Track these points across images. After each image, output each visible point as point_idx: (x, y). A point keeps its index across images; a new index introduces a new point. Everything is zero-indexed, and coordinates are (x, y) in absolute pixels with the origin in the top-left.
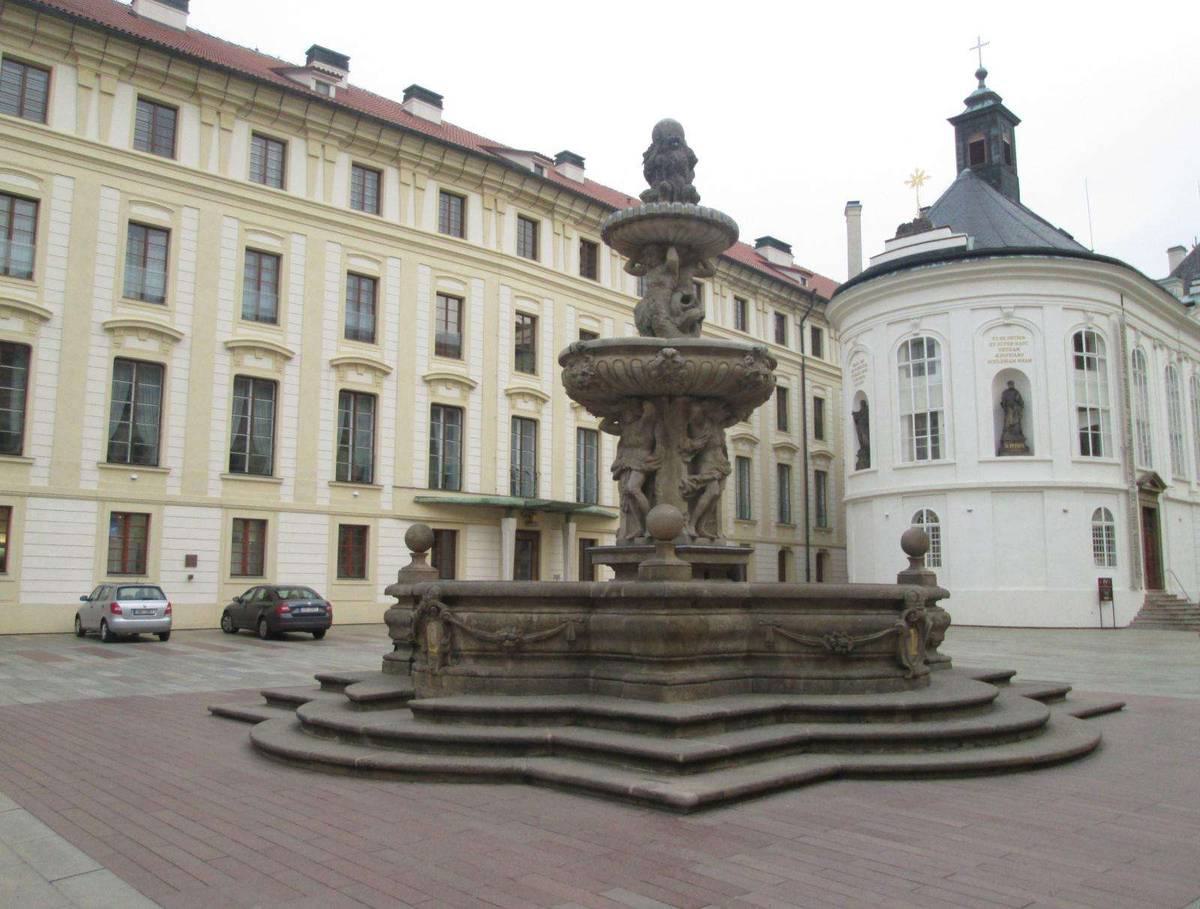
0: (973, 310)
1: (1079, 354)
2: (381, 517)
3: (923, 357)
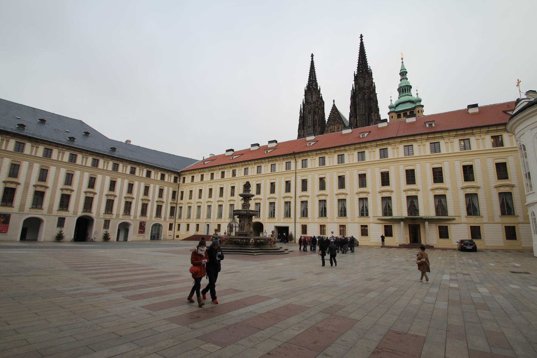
2: (370, 223)
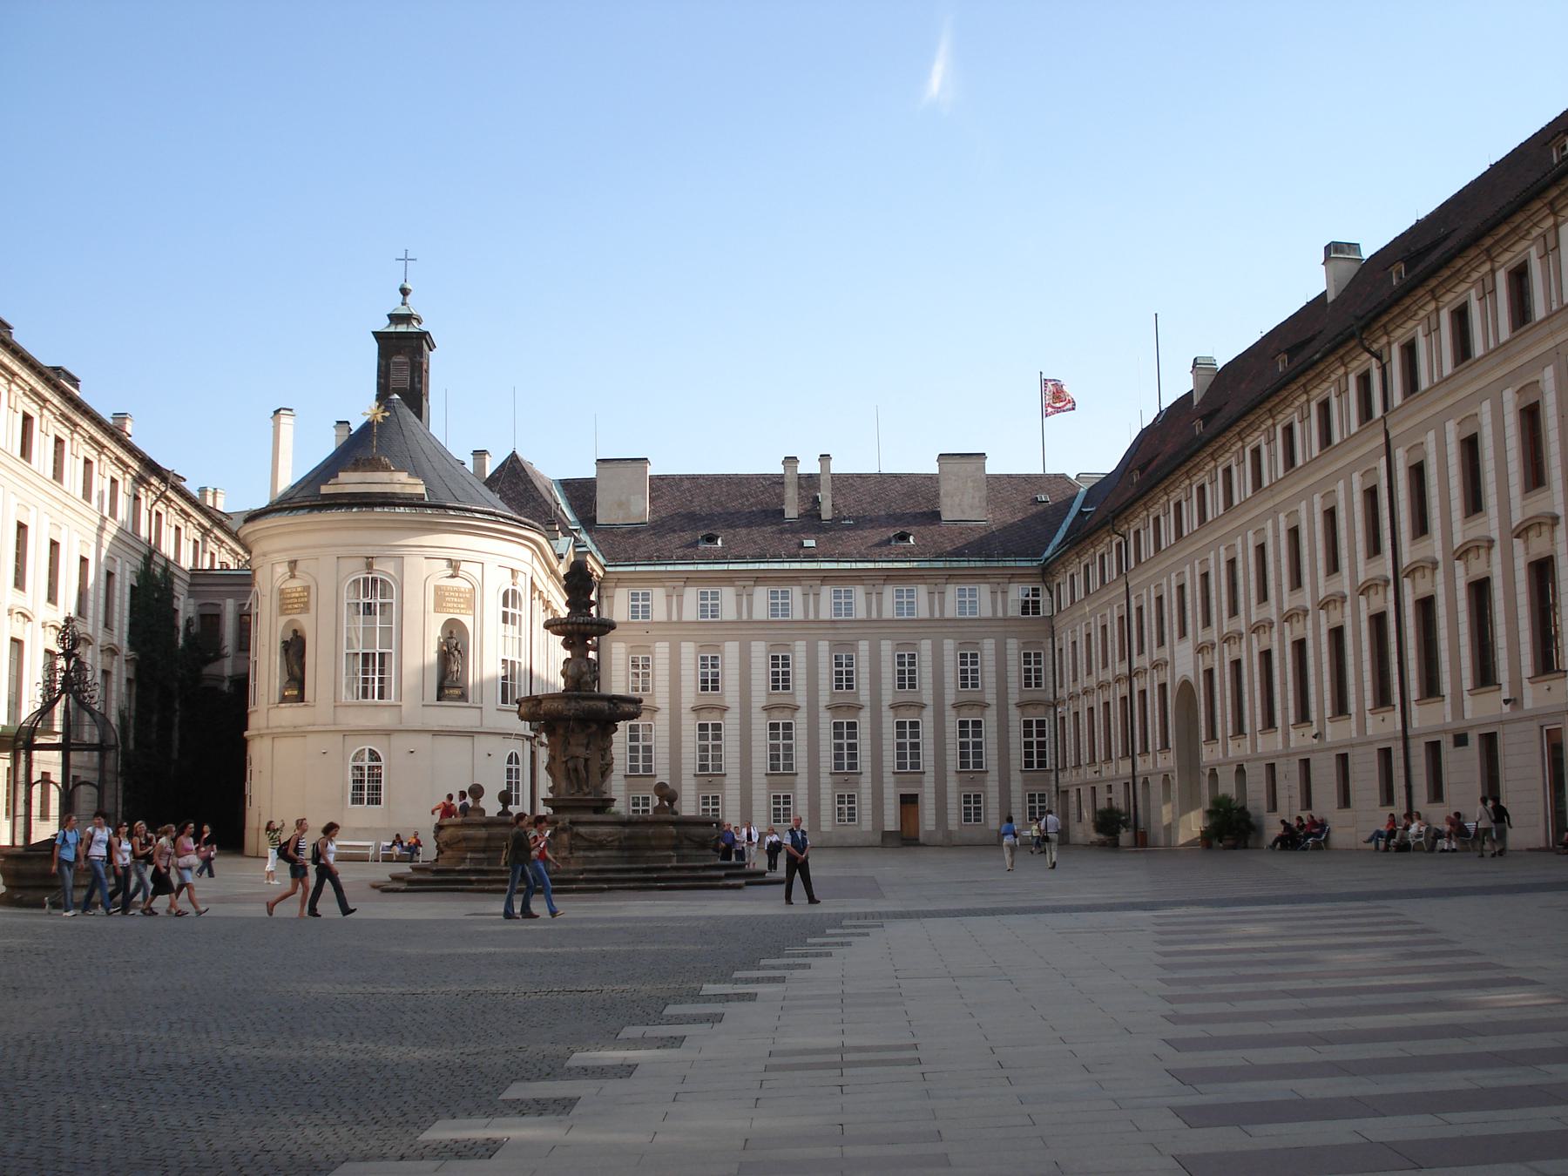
0: (426, 558)
1: (505, 609)
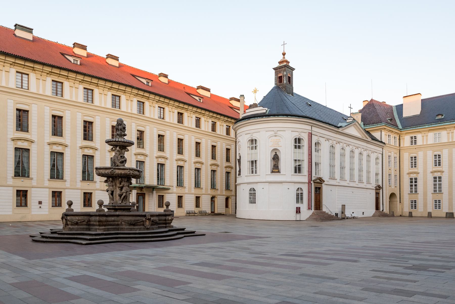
1: (296, 144)
3: (253, 144)
